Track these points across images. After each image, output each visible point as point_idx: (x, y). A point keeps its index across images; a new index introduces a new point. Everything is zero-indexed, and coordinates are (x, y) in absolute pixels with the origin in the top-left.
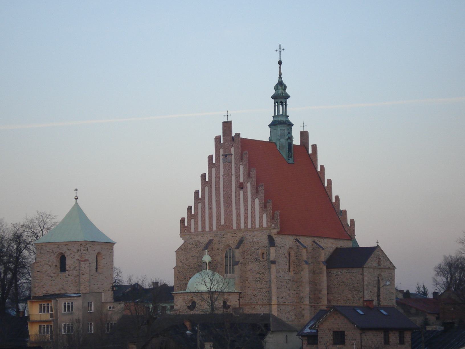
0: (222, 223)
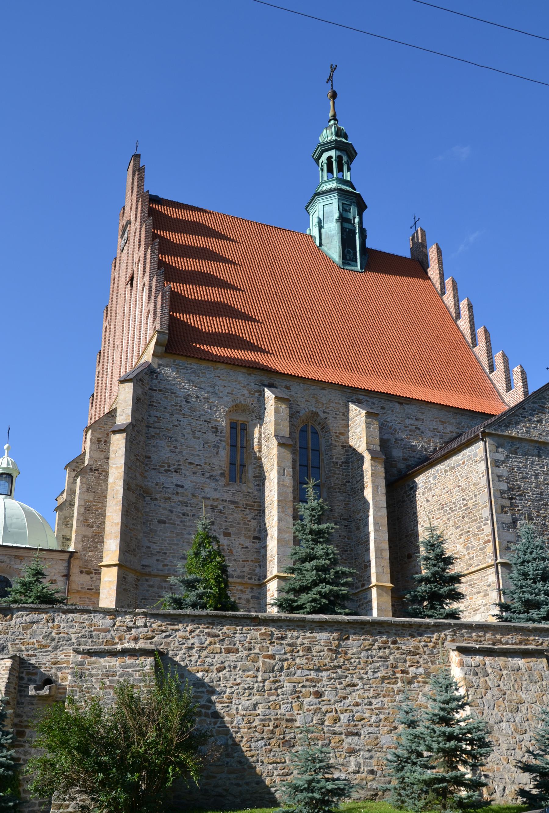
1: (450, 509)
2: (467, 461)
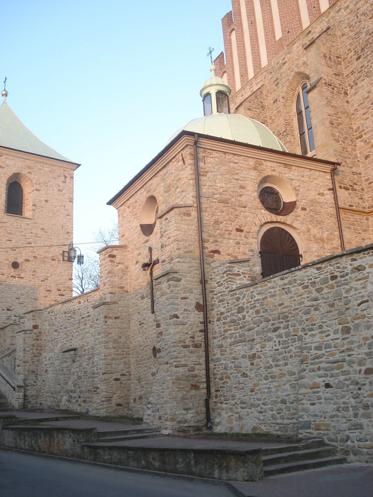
0: (279, 35)
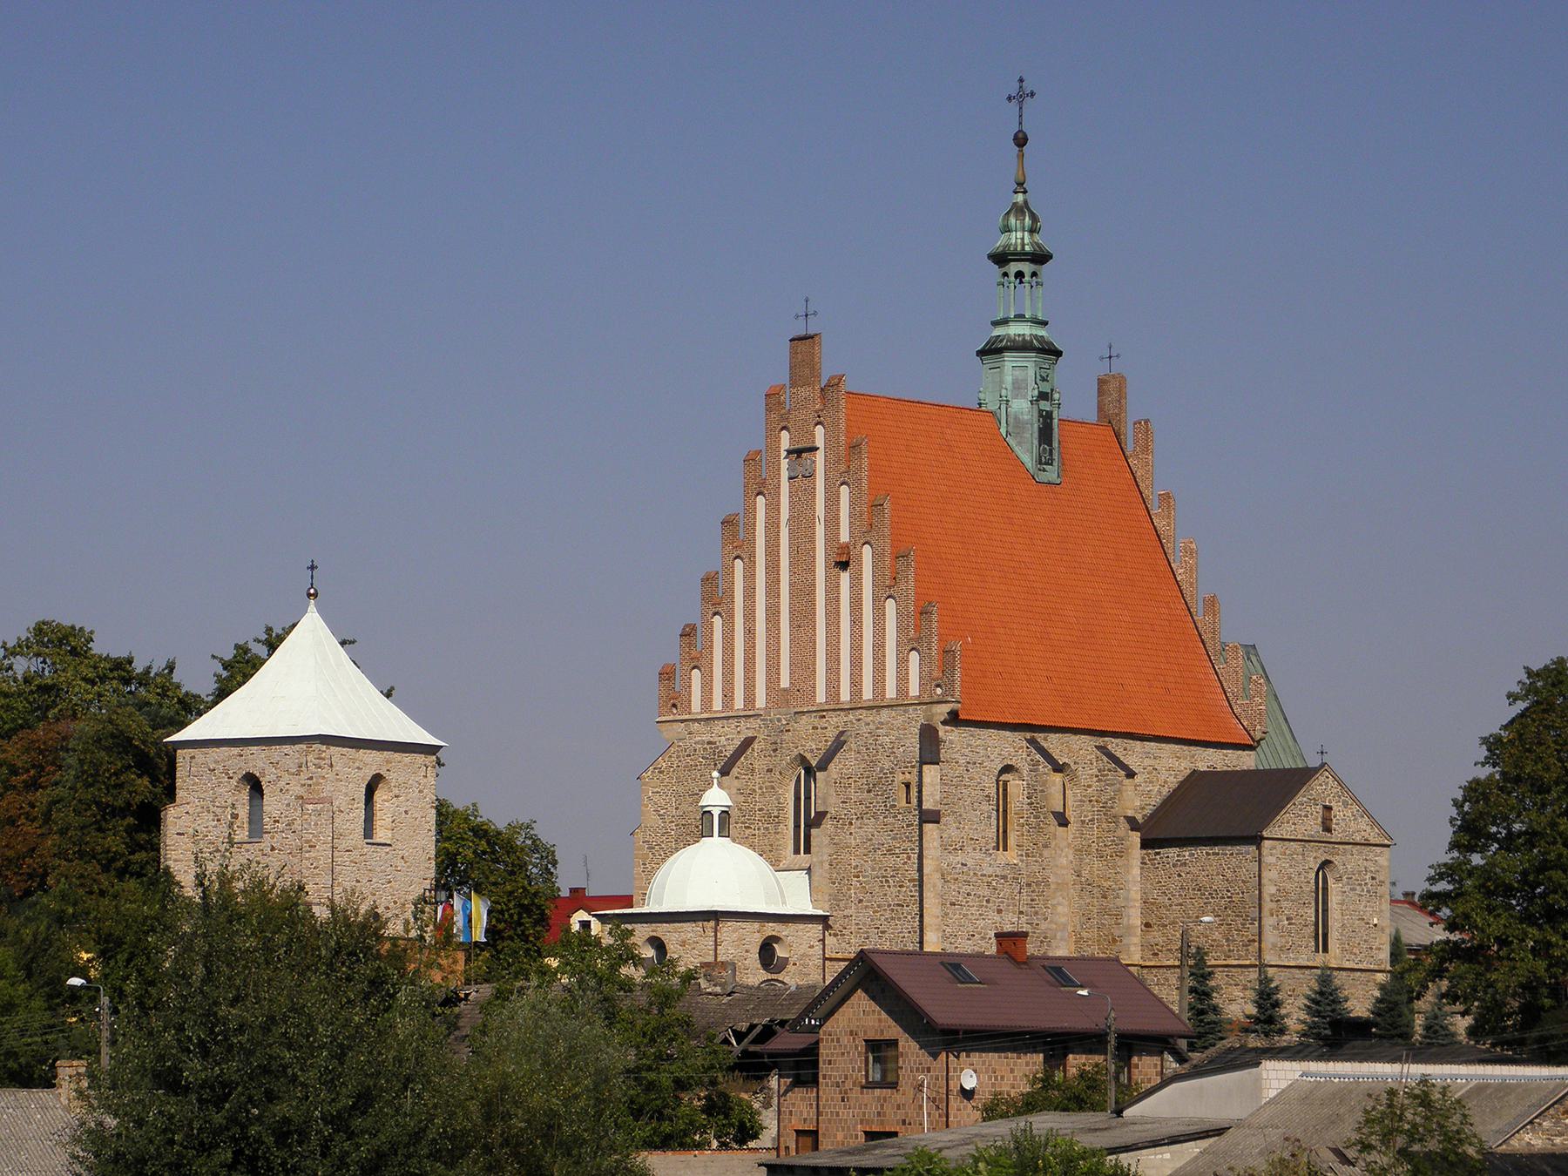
0: (785, 683)
1: (1209, 894)
2: (1237, 854)
